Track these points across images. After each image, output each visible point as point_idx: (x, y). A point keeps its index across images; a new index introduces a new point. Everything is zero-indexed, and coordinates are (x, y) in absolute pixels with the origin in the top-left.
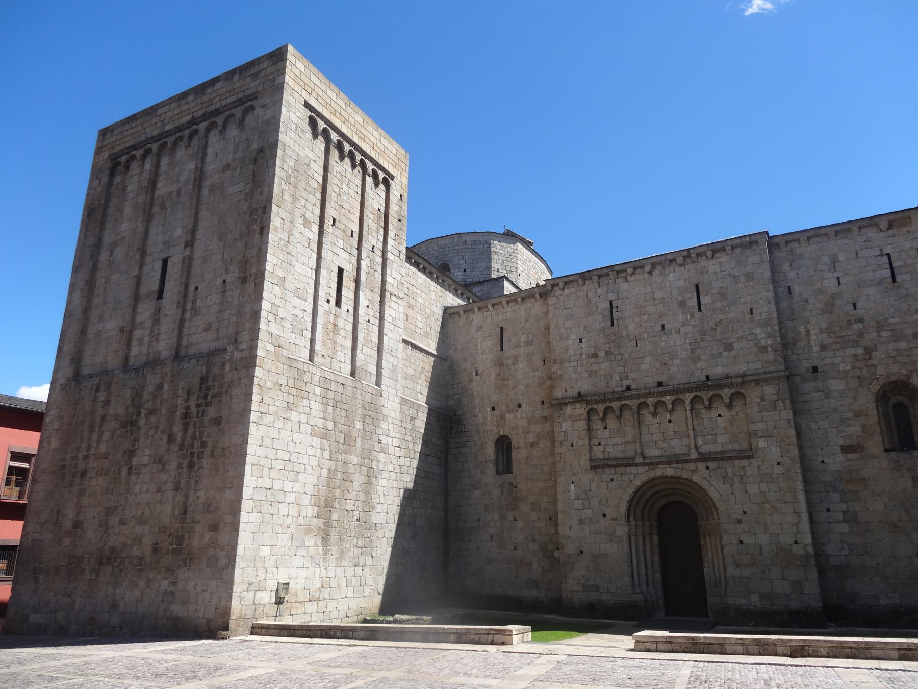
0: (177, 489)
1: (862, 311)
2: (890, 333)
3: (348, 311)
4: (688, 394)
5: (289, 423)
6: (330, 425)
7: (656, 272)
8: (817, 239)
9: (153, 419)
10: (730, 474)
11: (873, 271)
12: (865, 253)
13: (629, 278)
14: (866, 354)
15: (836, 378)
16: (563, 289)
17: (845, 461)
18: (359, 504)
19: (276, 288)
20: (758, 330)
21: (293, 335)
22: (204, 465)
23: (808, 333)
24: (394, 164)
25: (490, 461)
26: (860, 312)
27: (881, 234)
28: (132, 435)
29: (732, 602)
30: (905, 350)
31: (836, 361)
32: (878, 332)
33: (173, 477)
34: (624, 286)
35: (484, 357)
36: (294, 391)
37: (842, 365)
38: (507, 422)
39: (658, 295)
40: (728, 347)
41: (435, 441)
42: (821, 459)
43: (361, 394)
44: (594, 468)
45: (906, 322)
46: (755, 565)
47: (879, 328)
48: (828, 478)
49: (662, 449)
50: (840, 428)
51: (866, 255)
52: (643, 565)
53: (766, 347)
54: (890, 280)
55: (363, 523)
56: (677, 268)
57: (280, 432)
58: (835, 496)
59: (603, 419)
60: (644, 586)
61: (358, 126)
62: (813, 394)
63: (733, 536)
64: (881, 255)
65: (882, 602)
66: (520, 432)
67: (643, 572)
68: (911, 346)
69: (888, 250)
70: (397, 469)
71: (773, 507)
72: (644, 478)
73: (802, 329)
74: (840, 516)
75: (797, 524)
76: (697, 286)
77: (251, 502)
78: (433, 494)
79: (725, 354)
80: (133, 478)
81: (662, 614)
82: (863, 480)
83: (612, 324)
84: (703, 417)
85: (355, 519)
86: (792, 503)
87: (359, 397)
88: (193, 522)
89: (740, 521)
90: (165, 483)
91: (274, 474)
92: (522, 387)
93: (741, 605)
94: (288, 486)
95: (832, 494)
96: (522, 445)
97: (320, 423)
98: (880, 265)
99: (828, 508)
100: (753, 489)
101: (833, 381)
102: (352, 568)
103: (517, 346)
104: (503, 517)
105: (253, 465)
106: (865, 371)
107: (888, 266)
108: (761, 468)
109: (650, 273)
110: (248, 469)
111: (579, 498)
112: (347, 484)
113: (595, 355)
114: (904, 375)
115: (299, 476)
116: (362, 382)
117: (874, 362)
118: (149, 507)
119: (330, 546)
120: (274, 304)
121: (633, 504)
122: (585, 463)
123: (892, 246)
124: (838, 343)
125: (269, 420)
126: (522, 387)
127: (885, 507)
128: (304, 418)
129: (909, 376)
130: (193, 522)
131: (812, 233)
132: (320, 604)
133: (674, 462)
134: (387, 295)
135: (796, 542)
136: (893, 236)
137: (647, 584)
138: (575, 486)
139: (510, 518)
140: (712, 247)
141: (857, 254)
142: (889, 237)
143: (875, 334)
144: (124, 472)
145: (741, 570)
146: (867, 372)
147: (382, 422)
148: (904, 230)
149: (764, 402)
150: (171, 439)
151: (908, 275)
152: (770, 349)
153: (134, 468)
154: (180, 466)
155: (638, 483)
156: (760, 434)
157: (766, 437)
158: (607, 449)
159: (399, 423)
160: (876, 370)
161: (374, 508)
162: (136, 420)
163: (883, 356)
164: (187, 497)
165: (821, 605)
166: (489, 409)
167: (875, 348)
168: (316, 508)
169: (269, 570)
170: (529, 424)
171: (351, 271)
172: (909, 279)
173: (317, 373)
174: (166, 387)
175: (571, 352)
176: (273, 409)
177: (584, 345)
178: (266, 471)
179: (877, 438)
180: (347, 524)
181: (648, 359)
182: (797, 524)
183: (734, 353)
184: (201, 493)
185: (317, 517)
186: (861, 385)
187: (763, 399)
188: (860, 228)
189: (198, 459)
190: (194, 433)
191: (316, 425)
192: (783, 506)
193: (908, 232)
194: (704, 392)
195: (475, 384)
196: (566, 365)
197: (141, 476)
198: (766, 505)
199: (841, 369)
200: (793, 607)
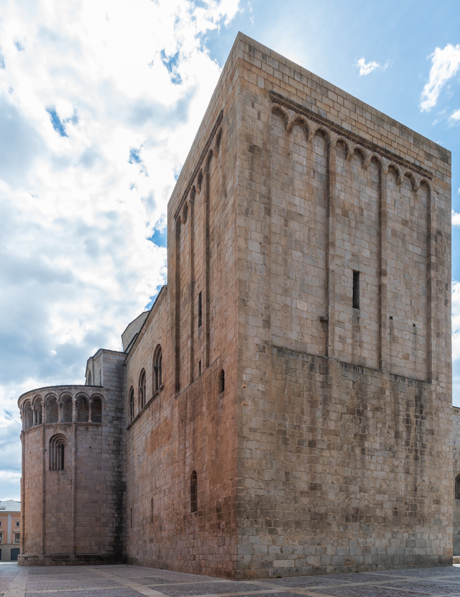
0: (407, 472)
9: (379, 414)
22: (426, 460)
28: (361, 422)
33: (403, 464)
80: (367, 457)
88: (422, 496)
90: (397, 467)
118: (385, 482)
130: (422, 496)
144: (358, 451)
150: (397, 435)
153: (367, 450)
154: (407, 457)
162: (363, 411)
164: (416, 480)
174: (388, 393)
184: (426, 478)
189: (421, 455)
190: (416, 436)
197: (374, 458)
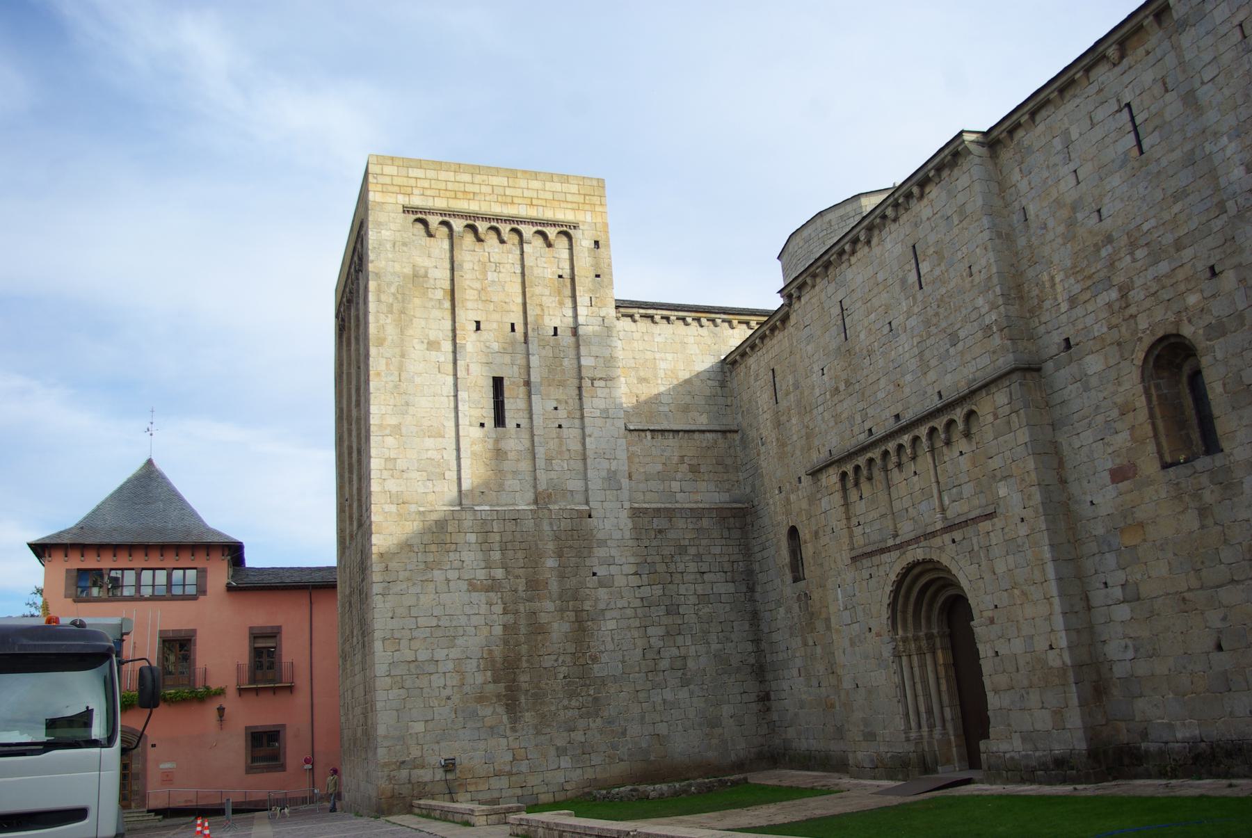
3: (518, 426)
4: (923, 428)
5: (431, 586)
6: (499, 573)
7: (875, 241)
8: (1044, 113)
10: (976, 548)
11: (1114, 142)
12: (1100, 115)
13: (853, 260)
14: (1122, 297)
15: (1093, 353)
16: (799, 298)
17: (1117, 496)
18: (568, 659)
19: (390, 441)
20: (980, 301)
21: (429, 484)
23: (1052, 278)
24: (575, 206)
25: (786, 564)
26: (1108, 223)
27: (1116, 68)
29: (995, 749)
30: (1167, 276)
31: (1089, 320)
32: (1132, 254)
34: (849, 274)
35: (765, 416)
36: (433, 548)
37: (1096, 327)
38: (792, 505)
39: (880, 277)
40: (954, 339)
41: (717, 550)
42: (1089, 498)
43: (551, 524)
44: (854, 559)
45: (1164, 224)
46: (1013, 688)
47: (1133, 246)
48: (1100, 530)
49: (913, 518)
50: (1106, 441)
52: (921, 699)
53: (989, 327)
54: (1135, 152)
55: (578, 680)
56: (894, 227)
57: (419, 597)
58: (1110, 559)
59: (857, 484)
60: (925, 729)
61: (501, 191)
62: (1070, 387)
63: (988, 646)
65: (1179, 736)
66: (804, 519)
67: (922, 709)
70: (637, 603)
71: (1024, 593)
72: (898, 568)
73: (1045, 277)
74: (1117, 593)
75: (1049, 618)
76: (914, 247)
77: (388, 680)
78: (721, 622)
79: (952, 351)
81: (957, 769)
82: (1141, 525)
83: (846, 339)
84: (946, 458)
85: (562, 676)
86: (1042, 583)
87: (546, 527)
89: (992, 621)
91: (416, 644)
92: (798, 453)
93: (1005, 753)
94: (440, 654)
95: (1107, 555)
96: (808, 537)
97: (481, 574)
99: (1104, 581)
100: (1000, 567)
101: (1090, 357)
102: (565, 734)
103: (787, 394)
104: (805, 644)
105: (384, 639)
106: (1123, 329)
108: (1006, 530)
109: (868, 242)
110: (378, 645)
111: (846, 609)
112: (540, 638)
113: (837, 390)
114: (1172, 323)
115: (456, 641)
116: (551, 507)
117: (1133, 310)
119: (520, 712)
120: (388, 460)
121: (899, 607)
122: (846, 557)
123: (1130, 86)
124: (1088, 288)
125: (399, 588)
126: (798, 453)
127: (1170, 570)
128: (453, 575)
129: (1177, 323)
131: (1031, 105)
132: (513, 778)
133: (922, 538)
134: (586, 383)
135: (1051, 648)
136: (1130, 68)
137: (931, 727)
138: (841, 591)
139: (811, 643)
140: (914, 180)
143: (1128, 258)
145: (1000, 698)
146: (1126, 331)
147: (595, 550)
148: (1141, 51)
149: (998, 421)
152: (995, 329)
155: (893, 577)
156: (999, 476)
157: (1004, 478)
158: (867, 531)
159: (630, 543)
160: (1137, 324)
161: (595, 659)
165: (1081, 746)
166: (777, 492)
168: (489, 673)
169: (426, 747)
170: (810, 505)
171: (516, 375)
173: (468, 517)
175: (817, 392)
176: (402, 575)
177: (825, 378)
178: (404, 643)
179: (1151, 447)
180: (547, 684)
181: (882, 382)
182: (1049, 618)
183: (960, 346)
185: (495, 682)
186: (1122, 356)
187: (996, 417)
191: (474, 579)
192: (1033, 588)
194: (937, 420)
195: (762, 458)
196: (815, 412)
198: (1015, 590)
199: (1096, 334)
200: (1057, 752)
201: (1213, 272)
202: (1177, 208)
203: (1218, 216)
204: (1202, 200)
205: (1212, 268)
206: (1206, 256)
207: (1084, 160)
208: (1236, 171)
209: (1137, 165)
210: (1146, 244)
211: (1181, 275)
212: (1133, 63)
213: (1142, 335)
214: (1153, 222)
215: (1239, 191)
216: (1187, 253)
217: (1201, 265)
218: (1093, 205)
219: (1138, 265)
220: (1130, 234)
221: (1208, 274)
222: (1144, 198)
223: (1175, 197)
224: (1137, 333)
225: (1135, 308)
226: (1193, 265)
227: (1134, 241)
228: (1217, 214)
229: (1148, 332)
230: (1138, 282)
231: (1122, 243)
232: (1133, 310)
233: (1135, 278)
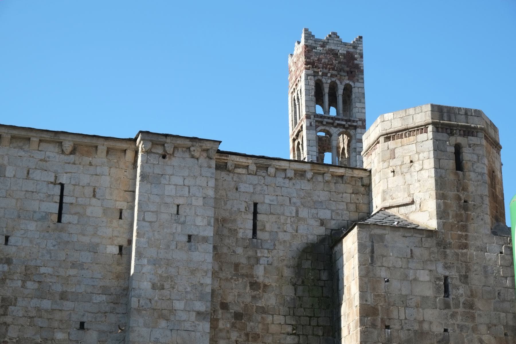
1: (14, 249)
2: (36, 285)
11: (41, 201)
12: (37, 175)
26: (11, 250)
27: (62, 156)
30: (46, 311)
32: (24, 282)
45: (58, 276)
47: (27, 276)
51: (38, 178)
54: (55, 218)
64: (55, 184)
68: (55, 306)
69: (63, 179)
98: (49, 195)
107: (57, 199)
117: (8, 319)
123: (69, 175)
136: (74, 164)
141: (28, 173)
142: (69, 163)
143: (20, 283)
148: (87, 160)
151: (76, 217)
160: (7, 331)
163: (21, 314)
167: (13, 302)
172: (76, 222)
188: (41, 141)
193: (90, 164)
201: (82, 325)
202: (72, 272)
203: (99, 294)
204: (92, 278)
205: (82, 324)
206: (82, 314)
207: (10, 195)
208: (145, 283)
209: (52, 225)
210: (39, 282)
211: (58, 316)
212: (77, 162)
213: (8, 340)
214: (50, 270)
215: (143, 295)
216: (68, 305)
217: (76, 318)
218: (5, 230)
219: (26, 292)
220: (27, 268)
221: (78, 326)
222: (49, 252)
223: (73, 264)
224: (5, 338)
225: (12, 320)
226: (70, 314)
227: (29, 274)
228: (100, 292)
229: (14, 341)
230: (21, 303)
231: (19, 271)
232: (8, 319)
233: (19, 299)
